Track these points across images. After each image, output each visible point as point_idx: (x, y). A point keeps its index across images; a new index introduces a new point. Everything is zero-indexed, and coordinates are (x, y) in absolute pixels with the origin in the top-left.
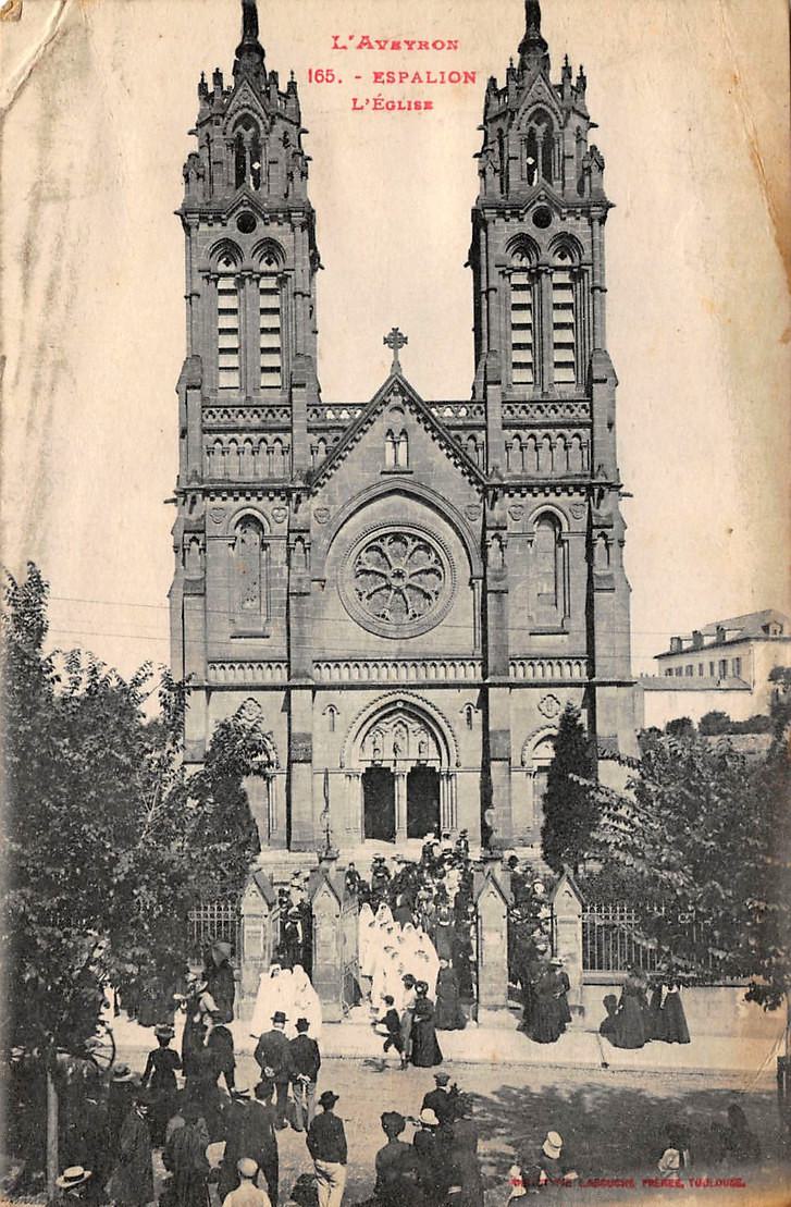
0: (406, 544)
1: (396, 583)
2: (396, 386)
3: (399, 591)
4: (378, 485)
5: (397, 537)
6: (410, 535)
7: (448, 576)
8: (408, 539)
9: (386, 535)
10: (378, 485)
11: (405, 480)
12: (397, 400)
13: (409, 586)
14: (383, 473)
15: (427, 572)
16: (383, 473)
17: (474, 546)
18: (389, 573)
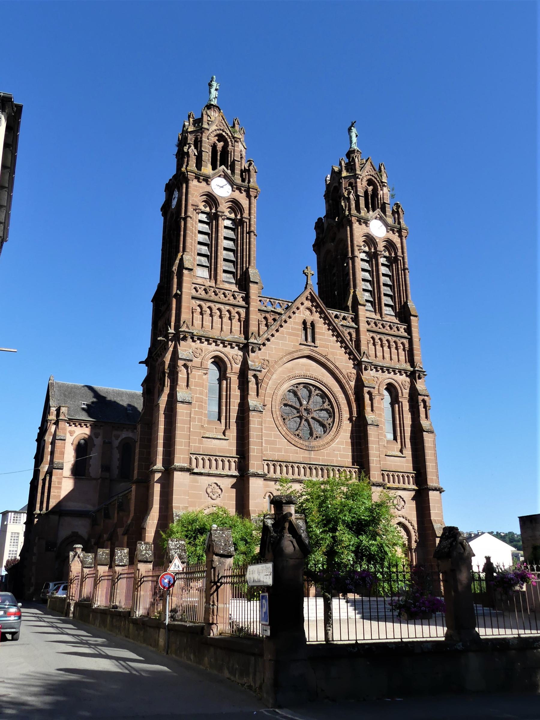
0: (310, 392)
1: (305, 414)
2: (309, 296)
3: (307, 420)
4: (297, 351)
5: (306, 386)
6: (314, 386)
7: (337, 415)
8: (311, 387)
9: (299, 384)
10: (297, 351)
11: (313, 351)
12: (308, 304)
13: (313, 418)
14: (300, 344)
15: (321, 410)
16: (300, 344)
17: (352, 398)
18: (302, 409)
